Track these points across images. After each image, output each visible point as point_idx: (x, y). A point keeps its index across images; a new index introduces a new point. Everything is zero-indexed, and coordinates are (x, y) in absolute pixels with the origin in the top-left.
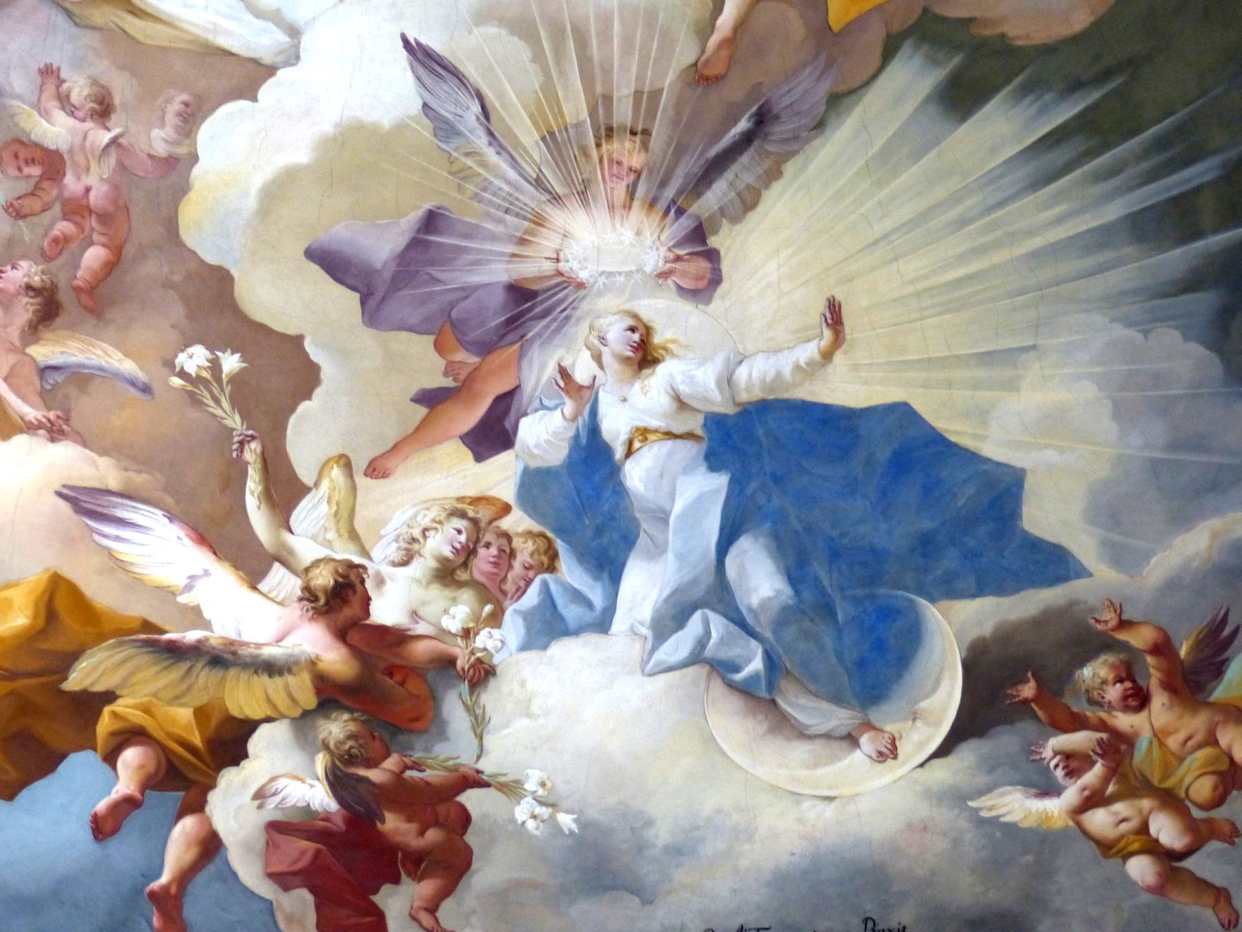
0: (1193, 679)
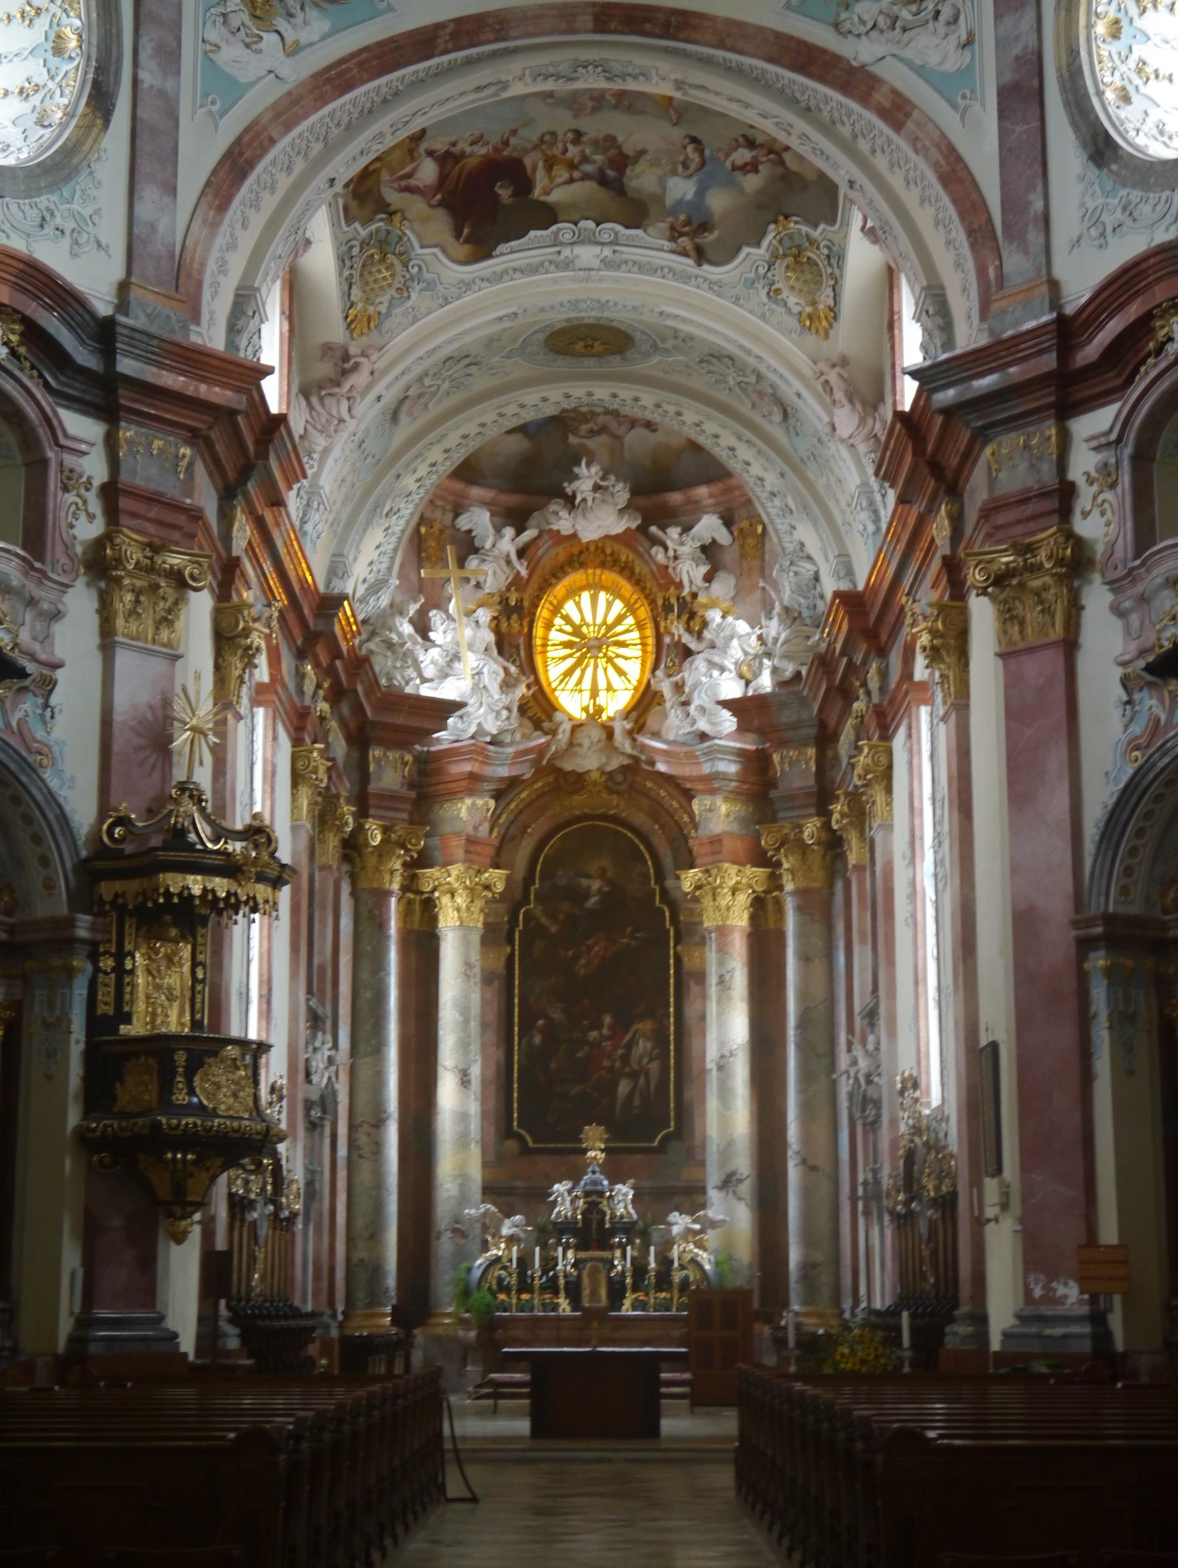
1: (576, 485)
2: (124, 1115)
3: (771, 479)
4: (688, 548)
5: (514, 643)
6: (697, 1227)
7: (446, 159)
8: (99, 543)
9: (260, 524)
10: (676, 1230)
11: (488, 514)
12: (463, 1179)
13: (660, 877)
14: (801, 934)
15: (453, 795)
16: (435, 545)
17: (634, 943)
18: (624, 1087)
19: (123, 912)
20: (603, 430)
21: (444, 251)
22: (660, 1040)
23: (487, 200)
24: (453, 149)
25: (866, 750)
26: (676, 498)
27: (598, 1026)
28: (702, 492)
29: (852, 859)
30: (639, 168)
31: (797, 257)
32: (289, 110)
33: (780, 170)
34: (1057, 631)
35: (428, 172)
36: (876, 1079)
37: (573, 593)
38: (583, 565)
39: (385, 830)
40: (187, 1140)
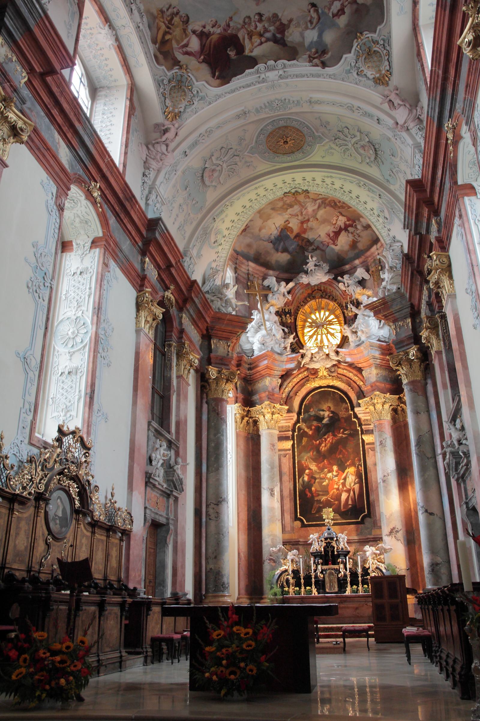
1: (308, 265)
6: (378, 552)
7: (202, 35)
10: (368, 554)
11: (275, 278)
14: (414, 402)
15: (263, 377)
17: (344, 436)
18: (344, 496)
21: (207, 82)
23: (225, 58)
24: (204, 30)
25: (435, 258)
26: (347, 267)
27: (331, 471)
28: (357, 262)
30: (290, 30)
31: (370, 54)
33: (355, 6)
35: (195, 44)
36: (464, 442)
37: (313, 311)
38: (314, 298)
39: (219, 372)
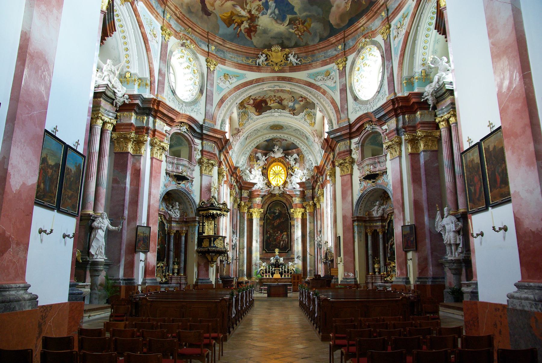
0: (303, 24)
2: (204, 248)
3: (305, 148)
4: (292, 159)
5: (265, 174)
7: (254, 100)
8: (200, 159)
9: (225, 156)
12: (256, 257)
13: (287, 210)
14: (309, 219)
15: (255, 197)
16: (253, 159)
18: (282, 243)
19: (203, 216)
20: (279, 141)
22: (287, 235)
23: (261, 106)
26: (290, 151)
28: (294, 150)
29: (317, 207)
31: (309, 114)
32: (230, 93)
34: (349, 172)
37: (274, 166)
40: (213, 252)
